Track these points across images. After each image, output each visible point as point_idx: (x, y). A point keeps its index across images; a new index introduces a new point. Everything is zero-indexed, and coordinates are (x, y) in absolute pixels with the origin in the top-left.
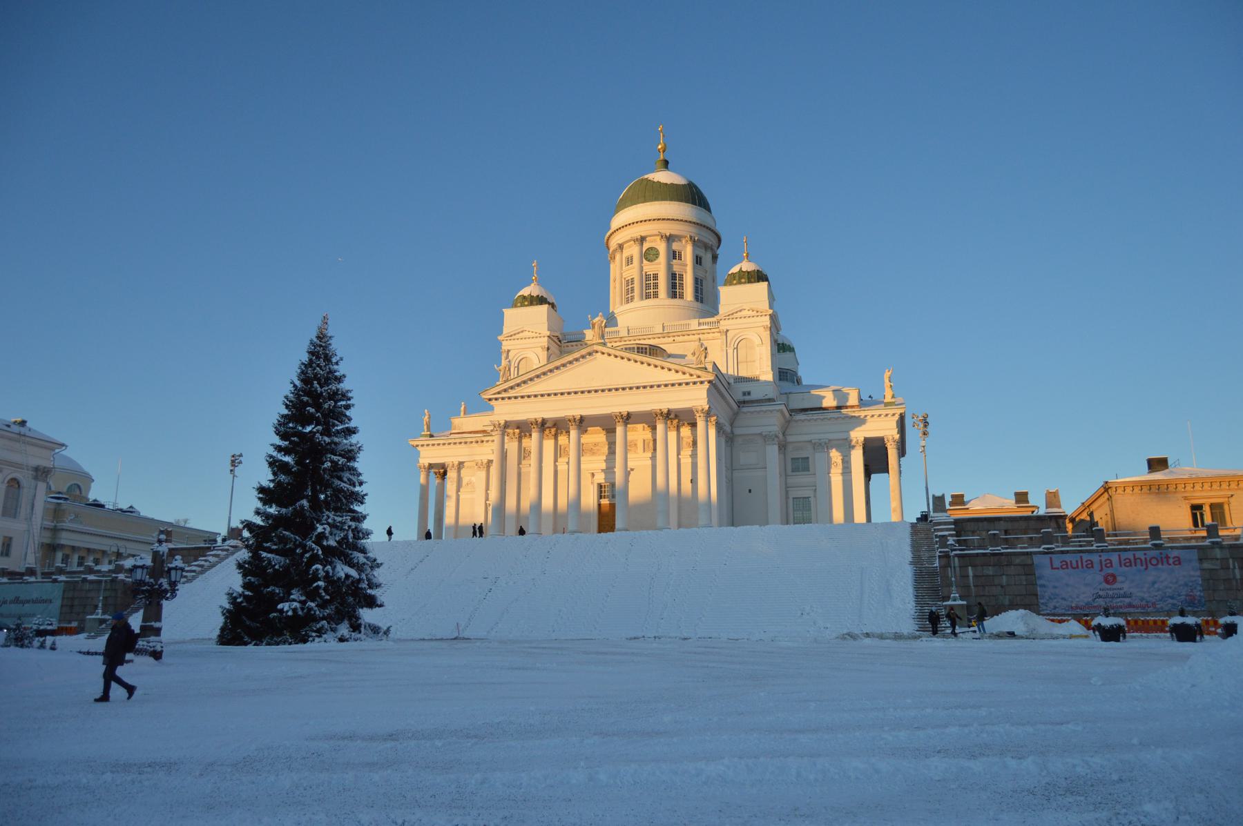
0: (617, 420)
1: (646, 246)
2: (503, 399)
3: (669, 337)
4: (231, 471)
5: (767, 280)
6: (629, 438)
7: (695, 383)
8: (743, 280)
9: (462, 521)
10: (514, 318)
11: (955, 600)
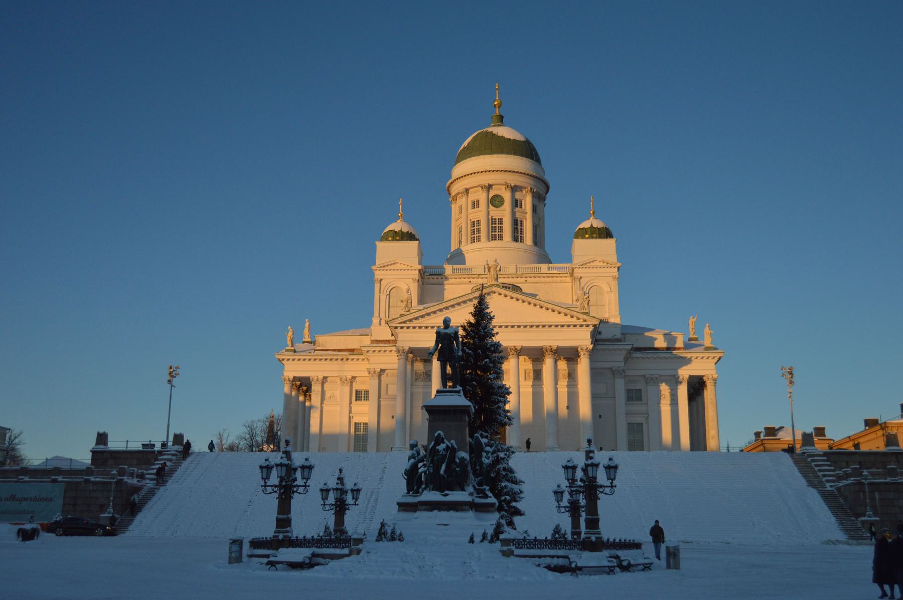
1: (492, 193)
2: (408, 327)
4: (169, 381)
7: (581, 326)
8: (594, 235)
9: (325, 430)
10: (386, 250)
11: (870, 517)
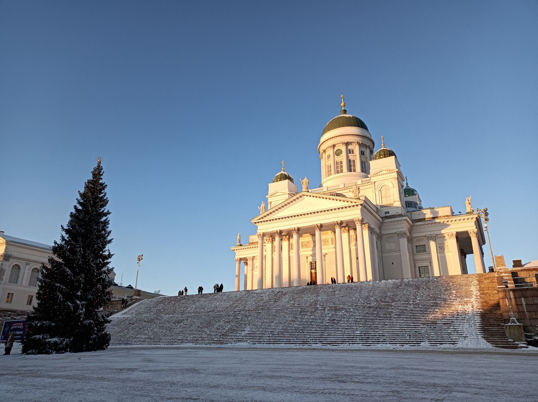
0: (315, 228)
1: (336, 149)
3: (347, 189)
4: (138, 263)
5: (394, 155)
6: (322, 238)
7: (353, 206)
8: (382, 156)
10: (273, 187)
